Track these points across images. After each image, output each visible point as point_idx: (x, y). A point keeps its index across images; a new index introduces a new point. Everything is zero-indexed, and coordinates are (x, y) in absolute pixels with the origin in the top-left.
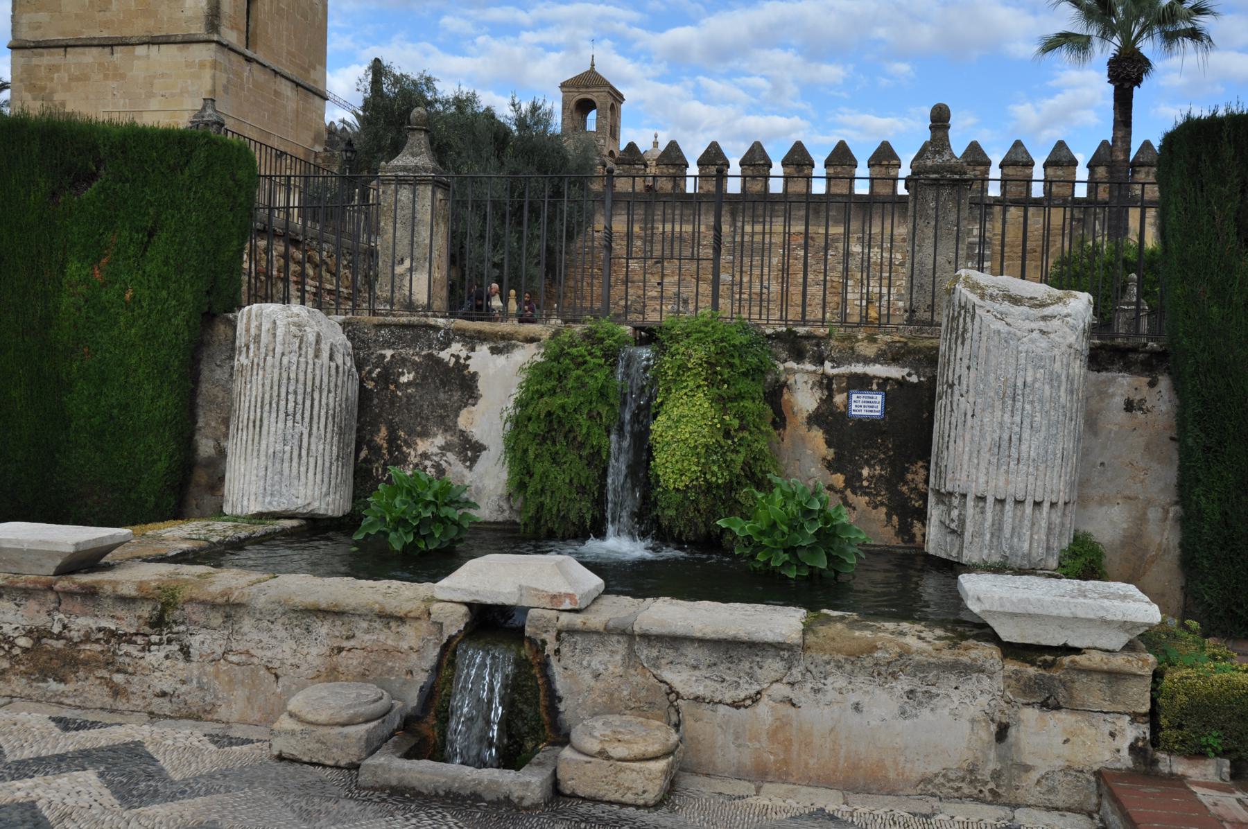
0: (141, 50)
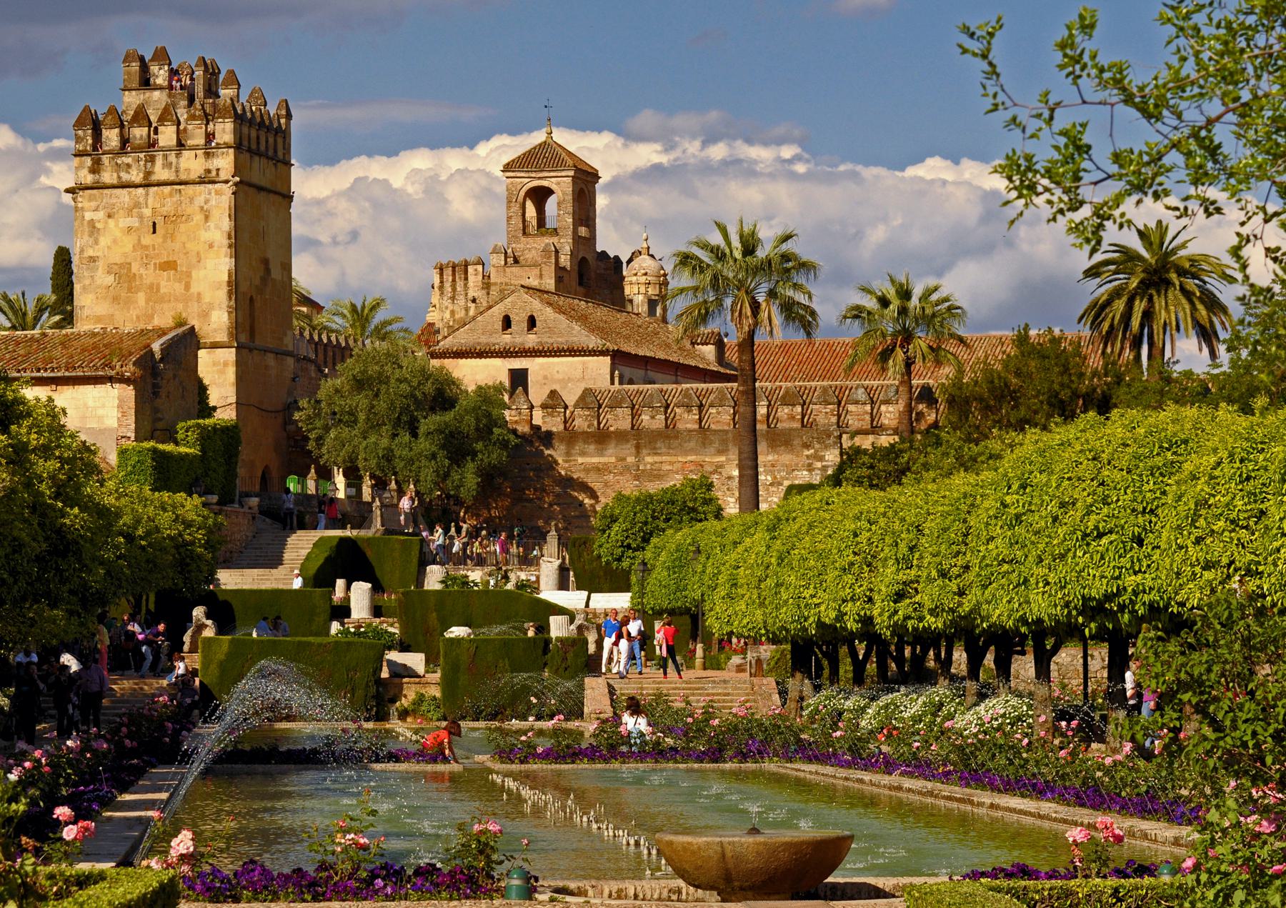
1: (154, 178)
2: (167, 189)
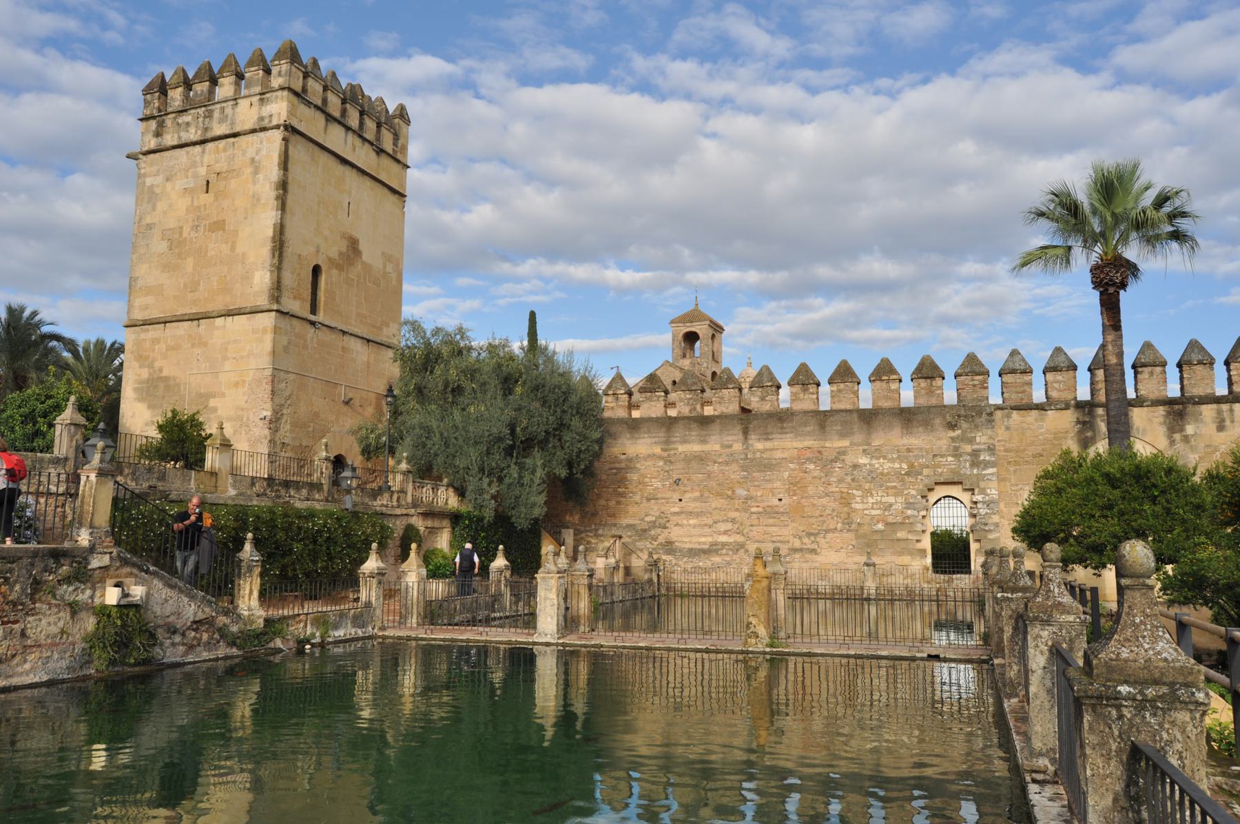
0: (219, 322)
2: (222, 144)
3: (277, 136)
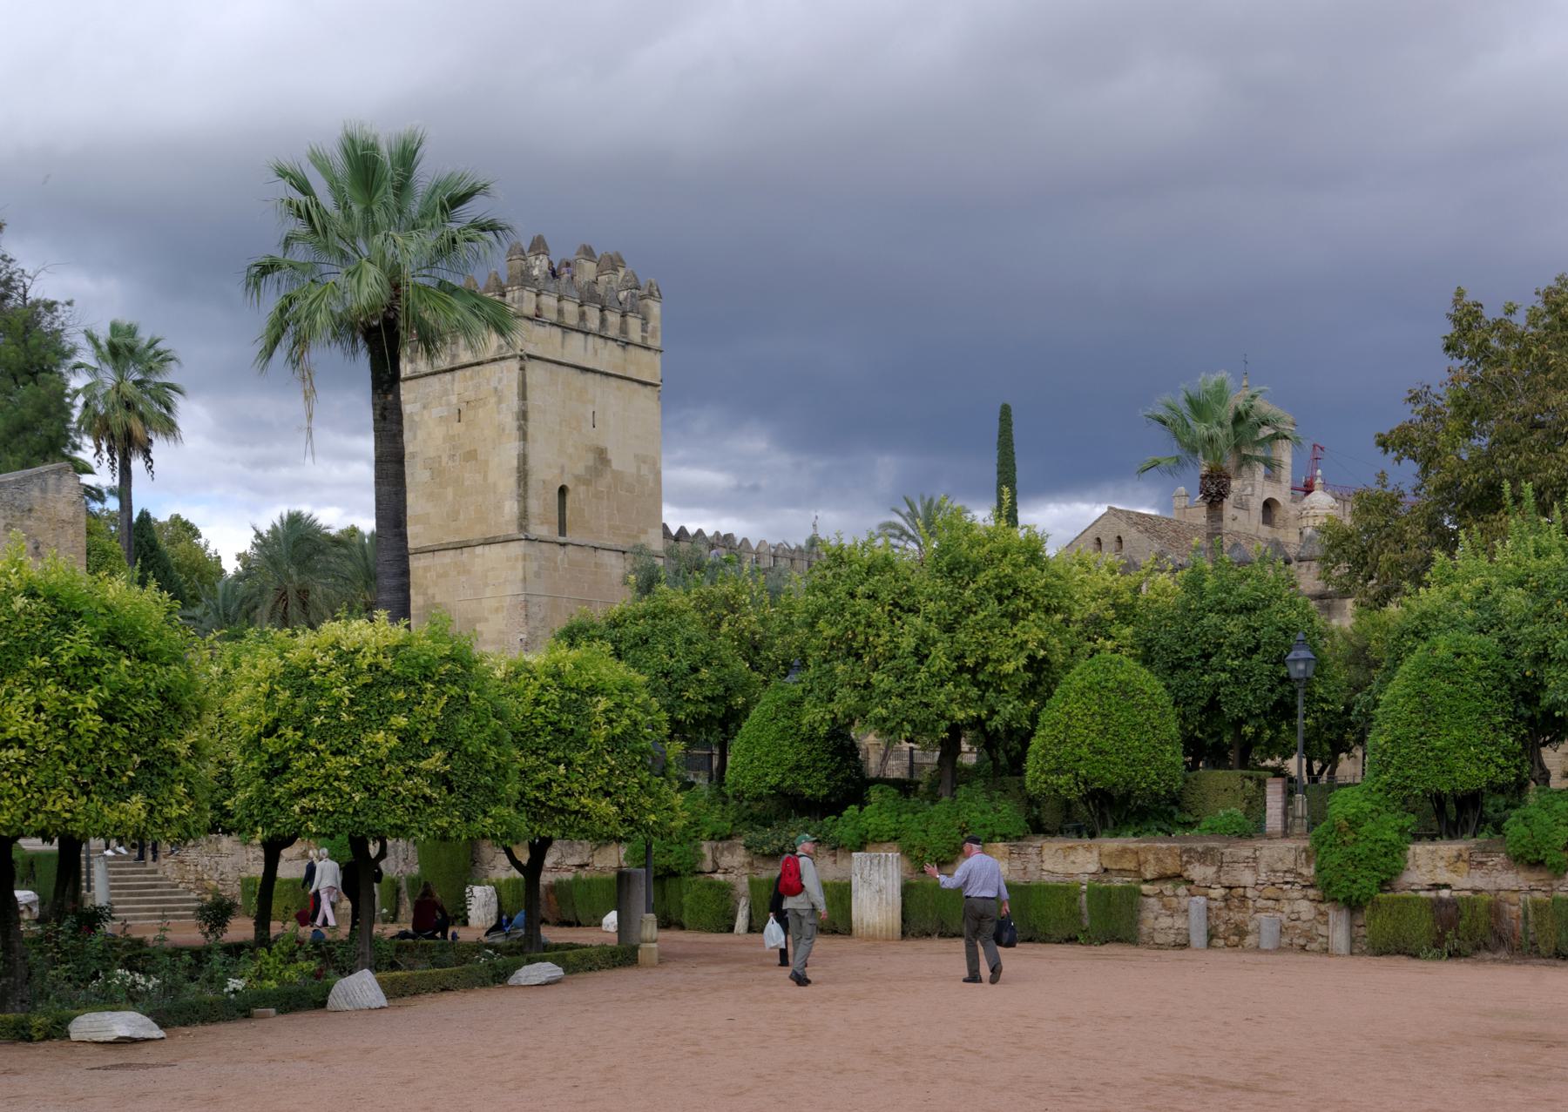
1: (458, 363)
2: (468, 372)
3: (514, 365)
